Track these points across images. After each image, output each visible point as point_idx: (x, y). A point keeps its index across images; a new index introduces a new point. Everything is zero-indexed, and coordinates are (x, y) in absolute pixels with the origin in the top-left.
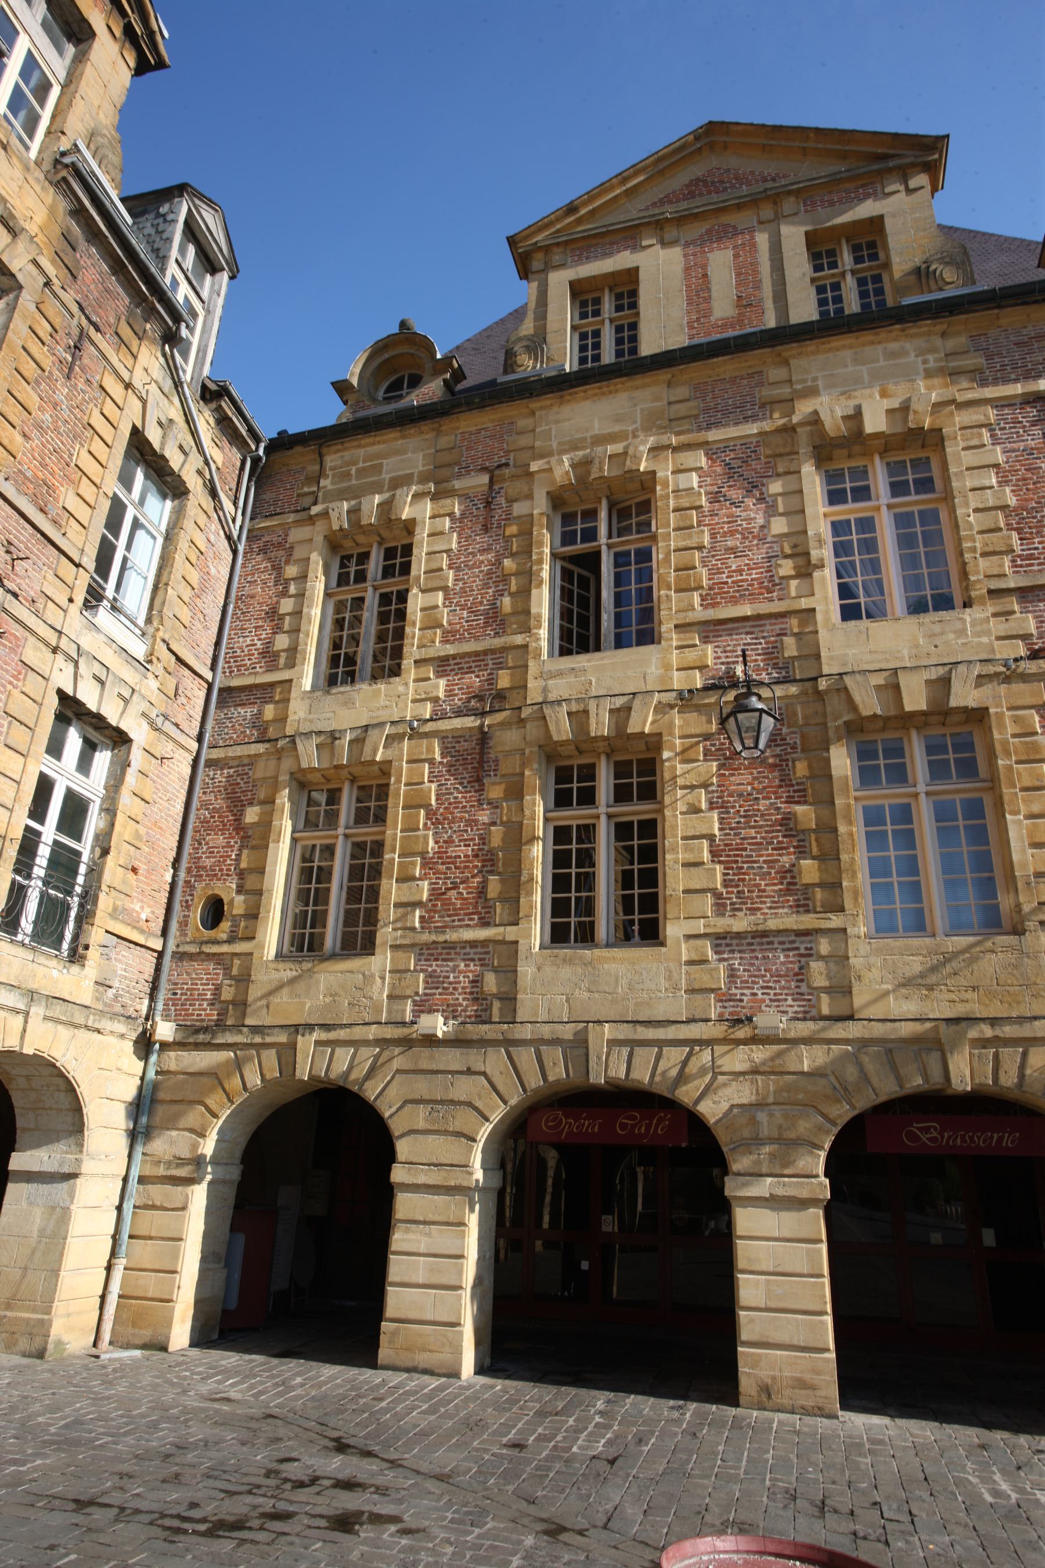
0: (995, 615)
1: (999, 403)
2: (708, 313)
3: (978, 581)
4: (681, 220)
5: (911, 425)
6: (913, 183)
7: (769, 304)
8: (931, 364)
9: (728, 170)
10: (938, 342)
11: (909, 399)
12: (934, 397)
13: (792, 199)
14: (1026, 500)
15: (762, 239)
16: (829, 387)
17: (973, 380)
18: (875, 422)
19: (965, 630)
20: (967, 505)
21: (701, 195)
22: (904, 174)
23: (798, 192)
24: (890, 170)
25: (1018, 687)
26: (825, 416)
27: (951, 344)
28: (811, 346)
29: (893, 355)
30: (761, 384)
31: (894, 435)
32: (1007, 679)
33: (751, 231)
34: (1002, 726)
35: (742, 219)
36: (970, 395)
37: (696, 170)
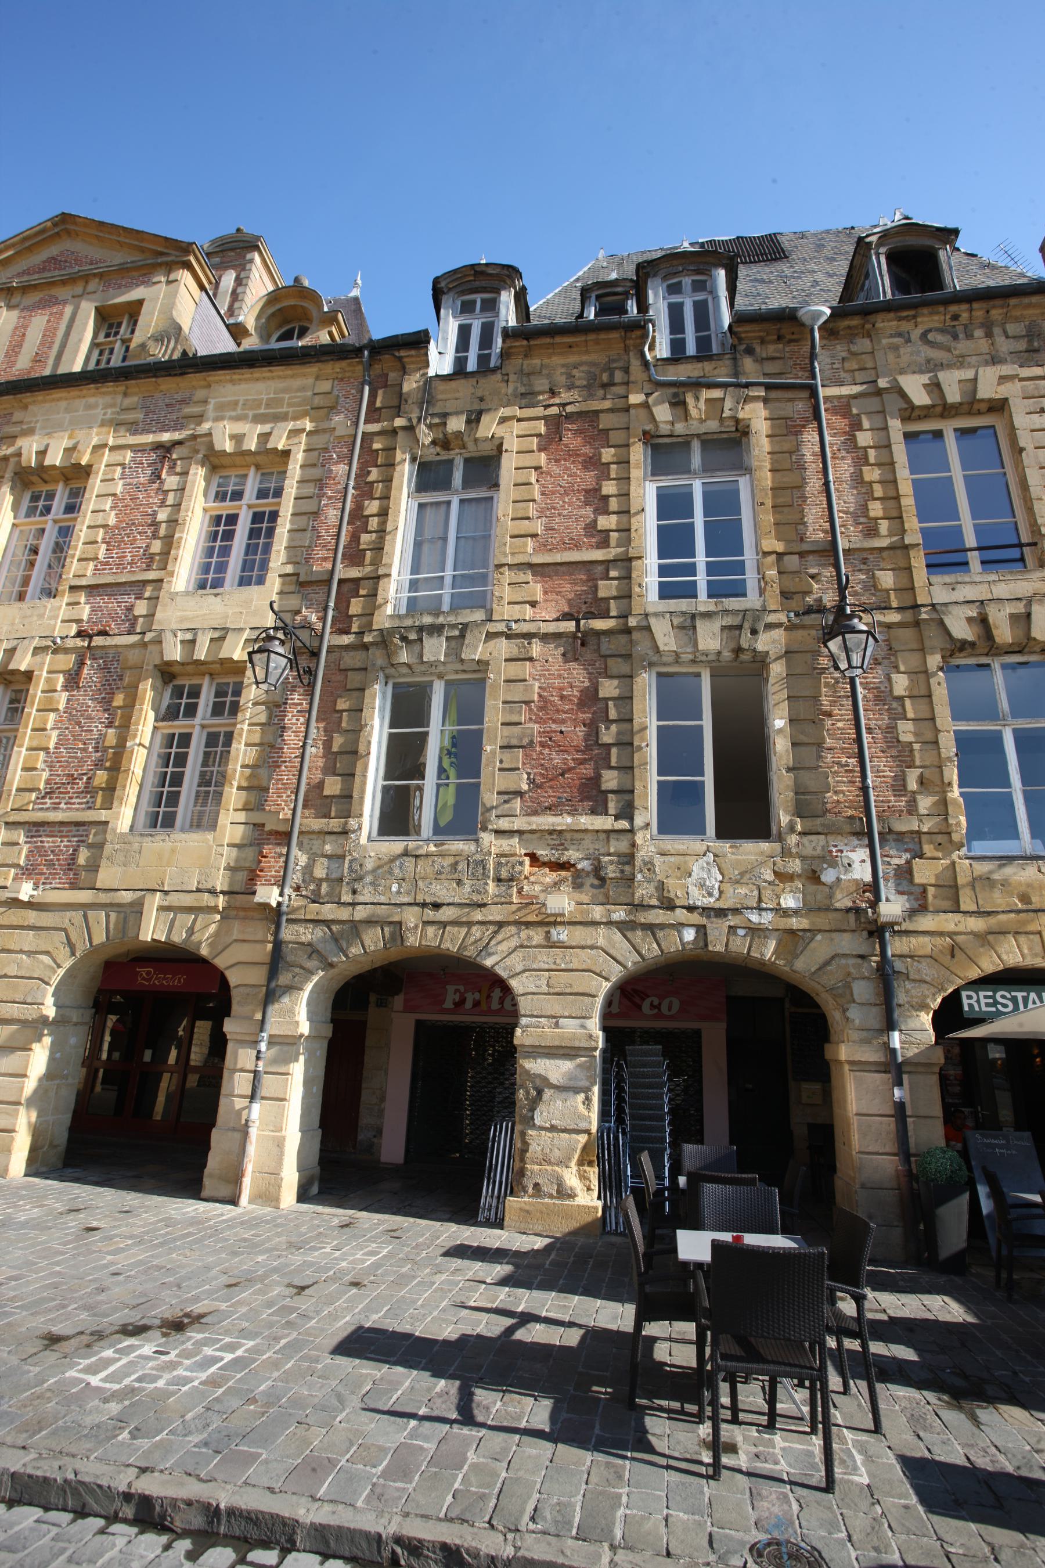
0: (68, 604)
1: (136, 448)
2: (14, 363)
3: (67, 579)
4: (26, 289)
5: (73, 461)
6: (172, 277)
7: (51, 362)
8: (108, 416)
9: (73, 253)
10: (119, 398)
11: (78, 442)
12: (95, 441)
13: (97, 280)
14: (121, 521)
15: (68, 310)
16: (43, 428)
17: (127, 430)
18: (55, 458)
19: (44, 614)
20: (84, 522)
21: (50, 270)
22: (170, 267)
23: (101, 276)
24: (160, 265)
25: (60, 657)
26: (24, 452)
27: (128, 402)
28: (40, 396)
29: (89, 407)
30: (8, 423)
31: (65, 467)
32: (55, 652)
33: (65, 302)
34: (38, 685)
35: (62, 292)
36: (121, 441)
37: (53, 250)
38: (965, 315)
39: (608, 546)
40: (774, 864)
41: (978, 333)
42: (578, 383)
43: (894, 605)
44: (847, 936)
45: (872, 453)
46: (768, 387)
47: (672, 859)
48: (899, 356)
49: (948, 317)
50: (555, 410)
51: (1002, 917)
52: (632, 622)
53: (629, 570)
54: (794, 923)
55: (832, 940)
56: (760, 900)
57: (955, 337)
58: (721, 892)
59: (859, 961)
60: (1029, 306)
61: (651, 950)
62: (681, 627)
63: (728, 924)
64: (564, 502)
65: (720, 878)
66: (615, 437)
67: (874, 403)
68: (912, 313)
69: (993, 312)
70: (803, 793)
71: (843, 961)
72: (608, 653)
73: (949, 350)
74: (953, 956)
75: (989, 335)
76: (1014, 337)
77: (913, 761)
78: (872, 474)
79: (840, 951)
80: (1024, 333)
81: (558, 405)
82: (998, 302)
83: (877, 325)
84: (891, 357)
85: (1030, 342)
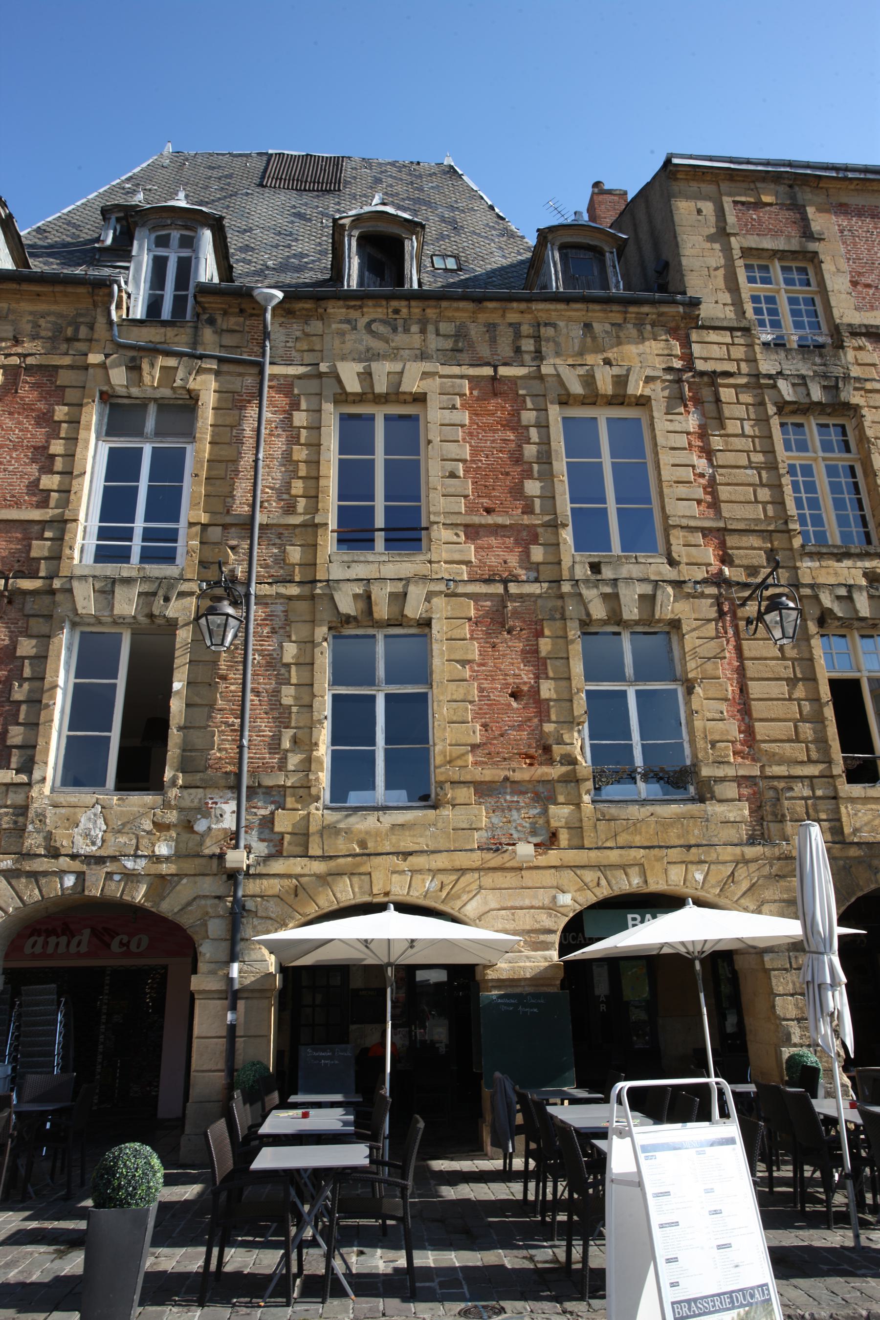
38: (404, 311)
39: (47, 507)
40: (154, 815)
41: (415, 328)
42: (43, 333)
43: (297, 579)
44: (208, 880)
45: (304, 432)
46: (221, 360)
47: (63, 811)
48: (344, 343)
49: (390, 310)
50: (15, 360)
51: (341, 861)
52: (57, 584)
53: (63, 532)
54: (165, 868)
55: (196, 883)
56: (137, 848)
57: (395, 330)
58: (103, 841)
59: (216, 901)
60: (458, 309)
61: (32, 894)
62: (102, 592)
63: (105, 870)
64: (11, 457)
65: (104, 827)
66: (71, 395)
67: (313, 385)
68: (358, 303)
69: (428, 311)
70: (190, 751)
71: (203, 902)
72: (31, 612)
73: (387, 342)
74: (296, 895)
75: (423, 331)
76: (444, 336)
77: (290, 722)
78: (300, 453)
79: (201, 893)
80: (452, 333)
81: (19, 355)
82: (432, 303)
83: (328, 310)
84: (337, 342)
85: (456, 342)
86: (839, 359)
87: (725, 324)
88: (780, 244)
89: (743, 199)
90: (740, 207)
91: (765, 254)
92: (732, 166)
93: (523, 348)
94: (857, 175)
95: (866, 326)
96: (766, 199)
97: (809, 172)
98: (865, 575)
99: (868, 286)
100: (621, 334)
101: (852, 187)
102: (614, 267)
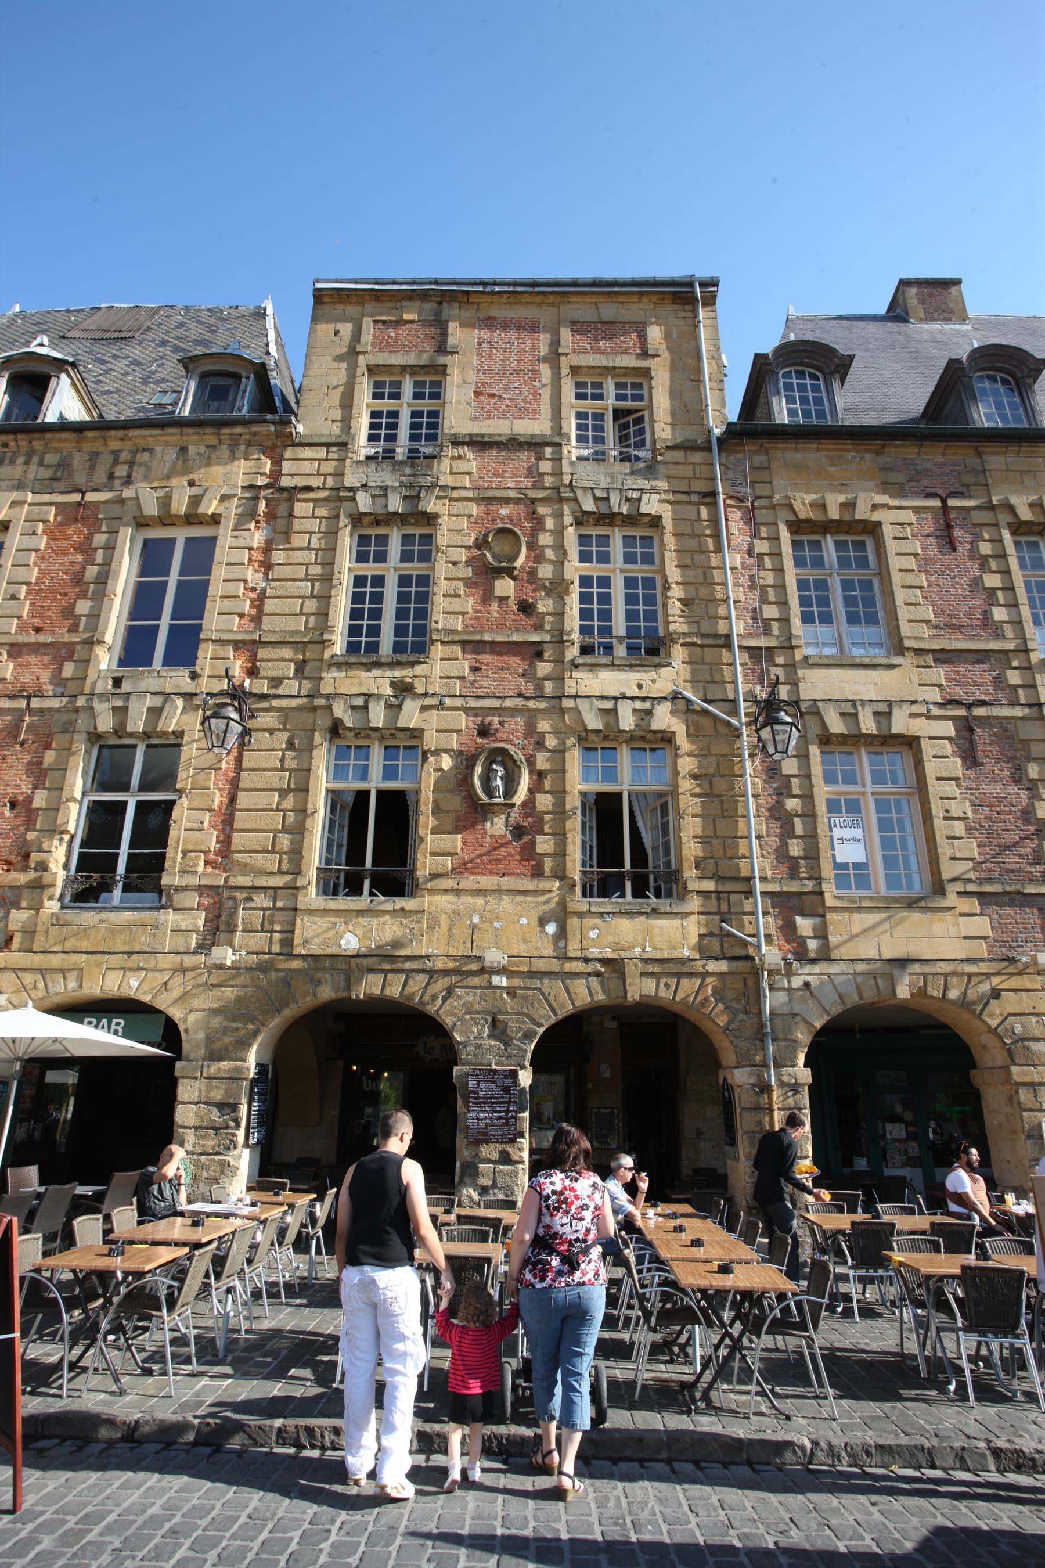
38: (12, 444)
41: (20, 460)
60: (61, 440)
69: (34, 443)
75: (27, 463)
82: (37, 435)
85: (56, 471)
86: (431, 469)
87: (323, 440)
88: (411, 359)
89: (385, 318)
90: (380, 326)
91: (395, 370)
92: (376, 287)
93: (117, 474)
94: (506, 289)
95: (470, 435)
96: (407, 317)
97: (455, 288)
98: (393, 684)
99: (492, 396)
100: (213, 456)
101: (504, 300)
102: (245, 391)
